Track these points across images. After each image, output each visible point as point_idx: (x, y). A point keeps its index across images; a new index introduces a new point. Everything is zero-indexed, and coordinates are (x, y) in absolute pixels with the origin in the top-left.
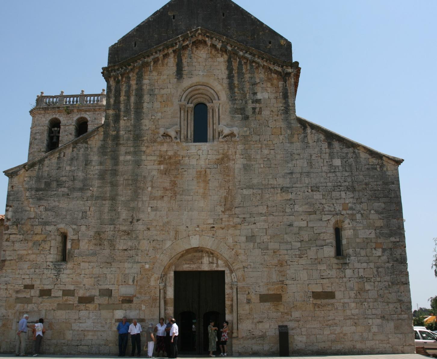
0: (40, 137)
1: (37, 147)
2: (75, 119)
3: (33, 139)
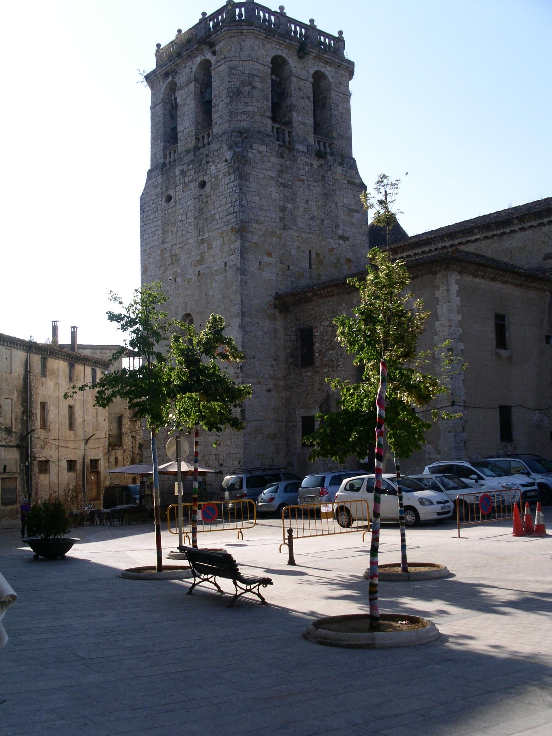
0: (260, 85)
1: (258, 105)
3: (245, 86)
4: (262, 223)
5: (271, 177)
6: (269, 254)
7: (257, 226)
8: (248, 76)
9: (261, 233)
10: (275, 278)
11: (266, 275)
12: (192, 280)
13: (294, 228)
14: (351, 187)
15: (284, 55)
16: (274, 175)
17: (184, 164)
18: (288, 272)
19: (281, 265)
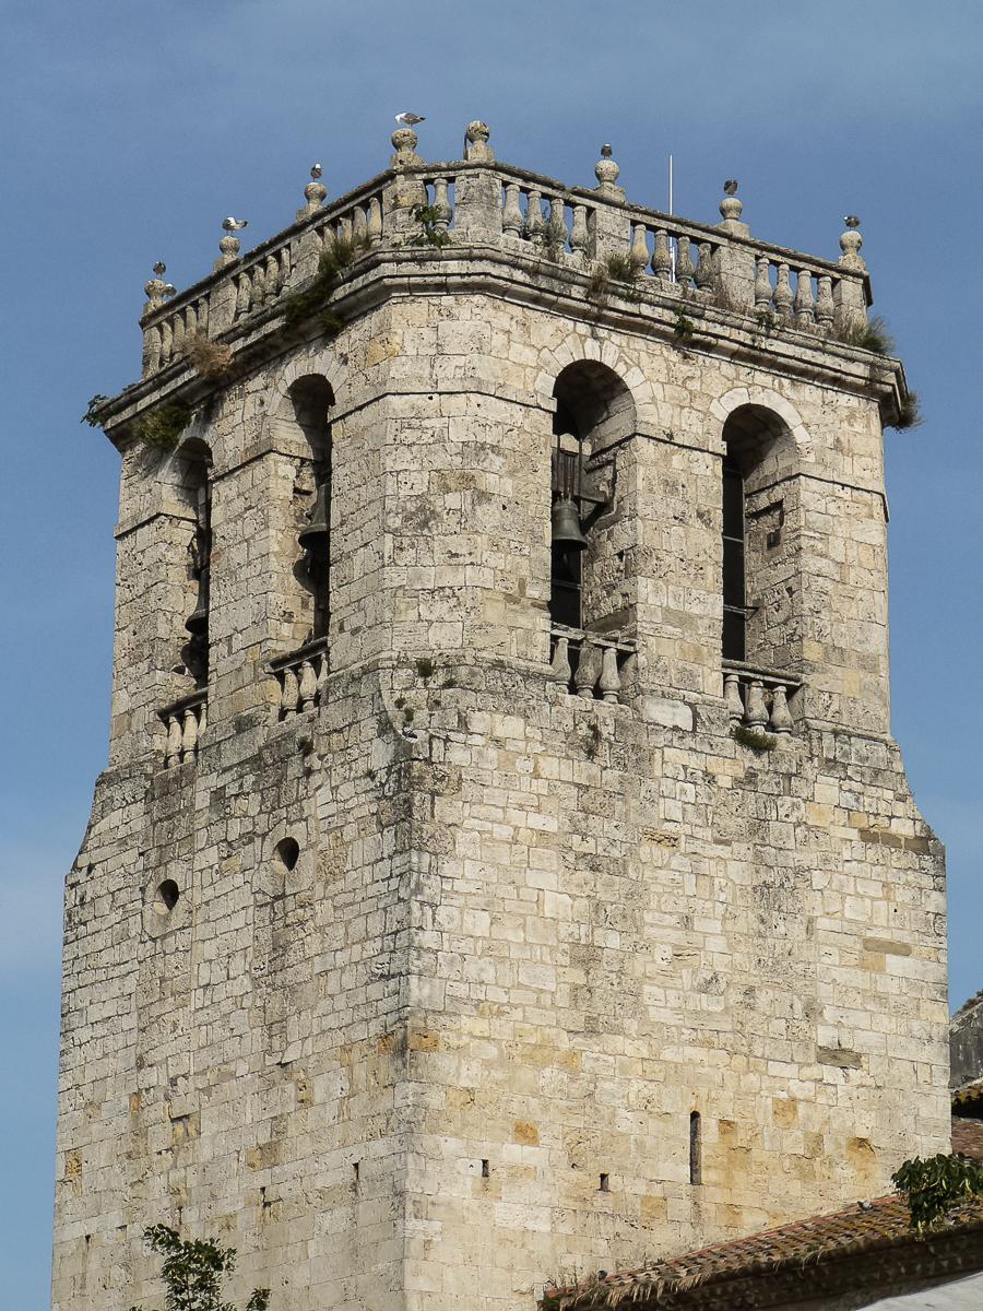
1: (498, 560)
2: (722, 411)
3: (447, 490)
4: (500, 1013)
5: (542, 833)
6: (525, 1133)
7: (480, 1026)
8: (461, 454)
9: (492, 1051)
10: (545, 1227)
11: (509, 1211)
12: (239, 1218)
13: (632, 1026)
14: (873, 853)
15: (608, 361)
16: (552, 826)
17: (225, 770)
18: (601, 1202)
19: (574, 1174)
